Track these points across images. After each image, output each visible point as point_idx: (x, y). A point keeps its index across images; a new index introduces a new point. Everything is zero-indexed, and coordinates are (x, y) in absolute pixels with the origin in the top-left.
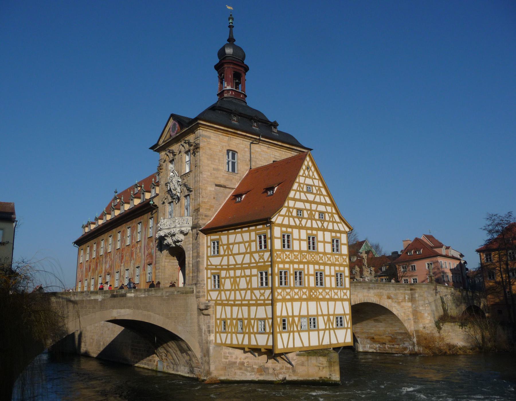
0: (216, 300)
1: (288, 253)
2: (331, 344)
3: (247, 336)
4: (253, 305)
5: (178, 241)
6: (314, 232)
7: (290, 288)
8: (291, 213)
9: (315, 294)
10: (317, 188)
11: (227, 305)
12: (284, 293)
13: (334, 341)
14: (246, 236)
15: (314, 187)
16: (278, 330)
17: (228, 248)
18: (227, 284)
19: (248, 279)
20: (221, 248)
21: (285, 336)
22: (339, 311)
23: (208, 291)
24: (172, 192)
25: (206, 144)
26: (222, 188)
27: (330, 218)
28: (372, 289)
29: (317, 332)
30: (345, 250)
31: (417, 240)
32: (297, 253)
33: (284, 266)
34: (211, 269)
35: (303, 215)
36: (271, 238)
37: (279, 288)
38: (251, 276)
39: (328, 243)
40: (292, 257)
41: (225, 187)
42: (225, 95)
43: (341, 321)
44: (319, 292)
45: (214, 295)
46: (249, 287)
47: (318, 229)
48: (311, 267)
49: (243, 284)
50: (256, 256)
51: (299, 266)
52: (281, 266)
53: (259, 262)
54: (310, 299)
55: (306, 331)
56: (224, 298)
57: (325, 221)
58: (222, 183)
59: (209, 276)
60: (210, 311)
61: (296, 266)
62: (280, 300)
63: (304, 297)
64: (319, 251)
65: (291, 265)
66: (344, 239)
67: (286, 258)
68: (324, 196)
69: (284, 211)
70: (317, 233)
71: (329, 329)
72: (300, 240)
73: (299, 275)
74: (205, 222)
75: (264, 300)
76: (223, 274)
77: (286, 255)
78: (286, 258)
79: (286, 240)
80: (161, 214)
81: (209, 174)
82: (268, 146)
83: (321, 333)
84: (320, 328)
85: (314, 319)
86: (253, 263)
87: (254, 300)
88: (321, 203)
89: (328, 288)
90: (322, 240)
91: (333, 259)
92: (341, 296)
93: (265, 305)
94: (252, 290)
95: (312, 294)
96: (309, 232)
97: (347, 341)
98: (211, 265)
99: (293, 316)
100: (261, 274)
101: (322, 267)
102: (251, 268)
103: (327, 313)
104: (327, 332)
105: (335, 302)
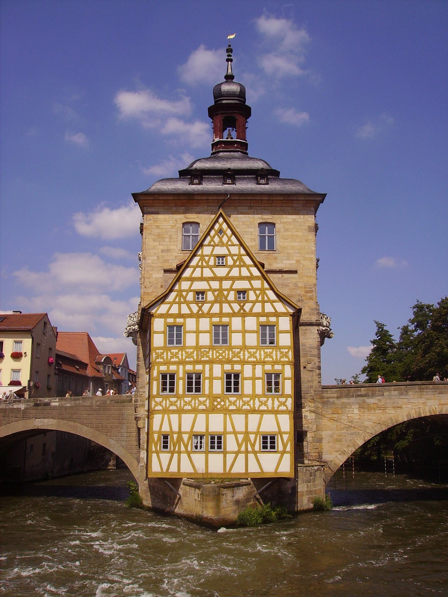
1: (174, 351)
7: (178, 396)
8: (185, 298)
9: (222, 403)
10: (235, 258)
12: (166, 403)
13: (254, 468)
15: (229, 258)
16: (154, 449)
21: (165, 457)
25: (152, 222)
27: (257, 297)
29: (221, 456)
30: (285, 340)
32: (192, 350)
33: (168, 368)
37: (158, 396)
44: (230, 402)
51: (194, 368)
52: (163, 368)
54: (213, 410)
61: (189, 367)
62: (158, 412)
63: (202, 407)
64: (234, 343)
67: (171, 357)
69: (172, 297)
70: (231, 320)
71: (247, 452)
77: (172, 353)
78: (171, 357)
79: (175, 333)
81: (156, 258)
82: (249, 205)
83: (230, 458)
84: (228, 449)
88: (241, 278)
89: (247, 396)
90: (240, 328)
91: (260, 355)
92: (273, 407)
95: (215, 403)
96: (216, 320)
97: (280, 470)
99: (180, 433)
101: (237, 368)
103: (243, 430)
104: (242, 456)
105: (262, 415)
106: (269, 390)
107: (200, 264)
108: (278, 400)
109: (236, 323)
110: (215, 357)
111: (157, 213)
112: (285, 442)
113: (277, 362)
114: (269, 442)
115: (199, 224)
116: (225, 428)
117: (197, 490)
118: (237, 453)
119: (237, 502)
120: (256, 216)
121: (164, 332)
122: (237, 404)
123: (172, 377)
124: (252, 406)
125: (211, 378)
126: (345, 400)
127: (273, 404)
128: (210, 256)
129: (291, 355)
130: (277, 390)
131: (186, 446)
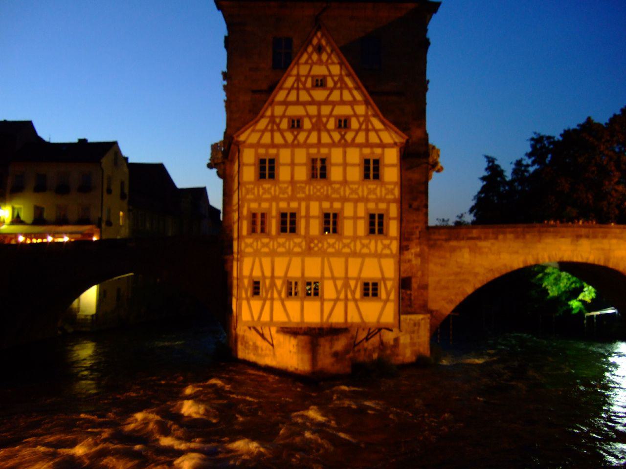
6: (324, 151)
8: (278, 125)
9: (320, 245)
21: (256, 304)
22: (371, 272)
27: (361, 125)
28: (587, 237)
30: (391, 174)
32: (286, 185)
33: (260, 205)
39: (354, 165)
44: (329, 244)
47: (333, 145)
52: (254, 206)
62: (249, 254)
63: (297, 250)
65: (274, 205)
67: (264, 193)
69: (263, 124)
78: (264, 193)
84: (326, 296)
88: (342, 102)
89: (348, 237)
92: (376, 251)
95: (312, 245)
96: (313, 151)
99: (273, 277)
101: (337, 205)
103: (342, 275)
106: (372, 231)
107: (295, 85)
108: (382, 243)
110: (312, 193)
112: (389, 289)
113: (381, 200)
114: (370, 290)
116: (323, 273)
118: (337, 300)
119: (336, 355)
122: (337, 246)
124: (353, 248)
126: (454, 243)
127: (376, 246)
128: (307, 76)
129: (397, 192)
130: (381, 232)
131: (279, 293)
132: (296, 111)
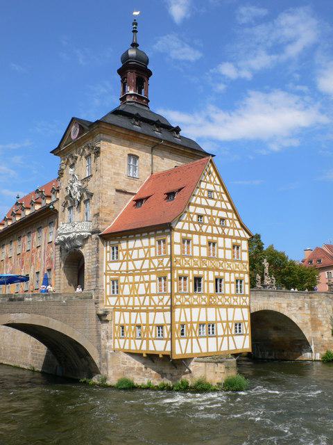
0: (115, 306)
1: (187, 259)
2: (229, 350)
3: (145, 341)
4: (152, 311)
5: (78, 247)
6: (215, 238)
8: (192, 219)
11: (126, 311)
12: (183, 299)
13: (232, 347)
14: (146, 242)
17: (127, 253)
18: (126, 290)
19: (147, 284)
20: (120, 254)
21: (183, 341)
22: (238, 318)
23: (107, 297)
24: (71, 197)
25: (106, 147)
26: (122, 195)
29: (215, 339)
31: (318, 249)
34: (110, 275)
35: (204, 220)
36: (171, 244)
37: (177, 294)
38: (149, 282)
40: (192, 263)
41: (125, 192)
42: (128, 100)
43: (240, 328)
45: (113, 300)
46: (148, 293)
47: (219, 235)
48: (211, 273)
49: (142, 290)
50: (156, 262)
52: (180, 272)
53: (158, 268)
54: (209, 305)
55: (205, 337)
56: (122, 303)
57: (226, 227)
58: (122, 187)
59: (108, 281)
60: (108, 317)
61: (196, 272)
63: (204, 303)
66: (245, 245)
68: (225, 202)
71: (228, 336)
72: (200, 246)
73: (198, 280)
74: (106, 228)
75: (163, 306)
76: (122, 279)
77: (185, 261)
80: (60, 219)
81: (110, 178)
85: (213, 326)
86: (152, 269)
87: (152, 306)
89: (227, 295)
93: (164, 311)
94: (151, 295)
96: (210, 238)
98: (110, 270)
99: (191, 323)
100: (160, 279)
101: (222, 274)
102: (149, 274)
104: (226, 338)
109: (220, 241)
111: (110, 142)
115: (138, 157)
117: (219, 364)
120: (174, 161)
121: (180, 244)
123: (185, 279)
125: (208, 282)
132: (200, 211)
